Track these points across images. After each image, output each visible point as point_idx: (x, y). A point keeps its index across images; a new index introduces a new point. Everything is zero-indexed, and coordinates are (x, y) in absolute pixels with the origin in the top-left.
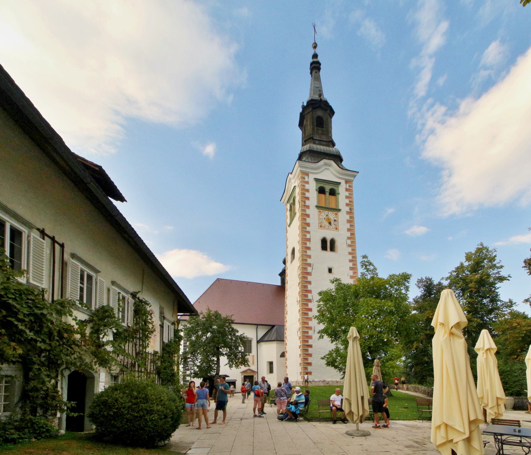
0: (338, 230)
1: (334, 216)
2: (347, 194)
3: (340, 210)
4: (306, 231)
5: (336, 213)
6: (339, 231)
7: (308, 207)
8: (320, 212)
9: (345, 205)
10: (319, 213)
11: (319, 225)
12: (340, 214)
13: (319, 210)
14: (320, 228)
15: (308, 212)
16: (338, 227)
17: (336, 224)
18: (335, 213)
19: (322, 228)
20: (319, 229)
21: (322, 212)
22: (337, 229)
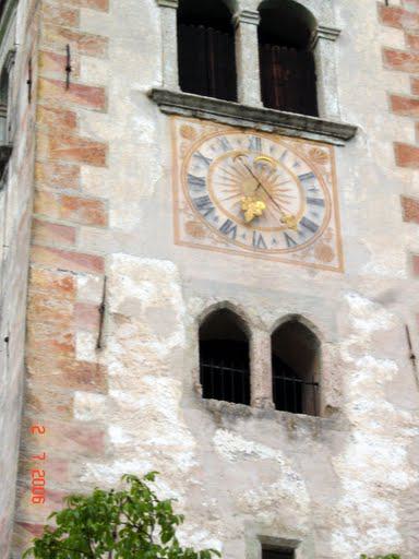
0: (335, 263)
1: (305, 169)
2: (396, 40)
3: (345, 134)
4: (73, 256)
5: (312, 152)
6: (341, 269)
7: (97, 98)
8: (185, 133)
9: (385, 104)
10: (180, 140)
11: (184, 219)
12: (341, 157)
13: (179, 123)
14: (183, 235)
15: (93, 125)
16: (333, 245)
17: (318, 222)
18: (307, 147)
19: (207, 242)
20: (178, 243)
21: (205, 139)
22: (325, 253)
